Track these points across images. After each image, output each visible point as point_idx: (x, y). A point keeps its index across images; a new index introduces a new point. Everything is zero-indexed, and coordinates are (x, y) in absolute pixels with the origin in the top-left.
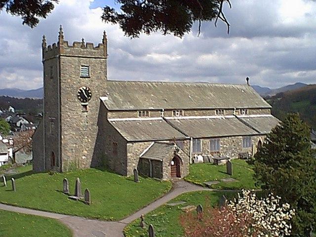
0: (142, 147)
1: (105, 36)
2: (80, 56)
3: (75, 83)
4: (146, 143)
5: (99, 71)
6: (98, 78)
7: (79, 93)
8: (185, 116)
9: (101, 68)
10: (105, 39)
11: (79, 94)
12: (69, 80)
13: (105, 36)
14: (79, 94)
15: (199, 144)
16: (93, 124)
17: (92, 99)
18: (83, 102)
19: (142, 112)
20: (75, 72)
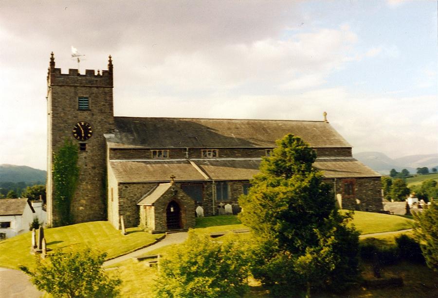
0: (139, 191)
1: (110, 61)
2: (76, 85)
3: (69, 117)
4: (145, 186)
5: (102, 103)
6: (102, 112)
7: (75, 129)
8: (220, 157)
9: (106, 100)
10: (111, 66)
11: (74, 131)
12: (62, 115)
13: (110, 61)
14: (74, 131)
15: (225, 189)
16: (94, 168)
17: (92, 137)
18: (80, 140)
19: (157, 151)
20: (70, 105)
